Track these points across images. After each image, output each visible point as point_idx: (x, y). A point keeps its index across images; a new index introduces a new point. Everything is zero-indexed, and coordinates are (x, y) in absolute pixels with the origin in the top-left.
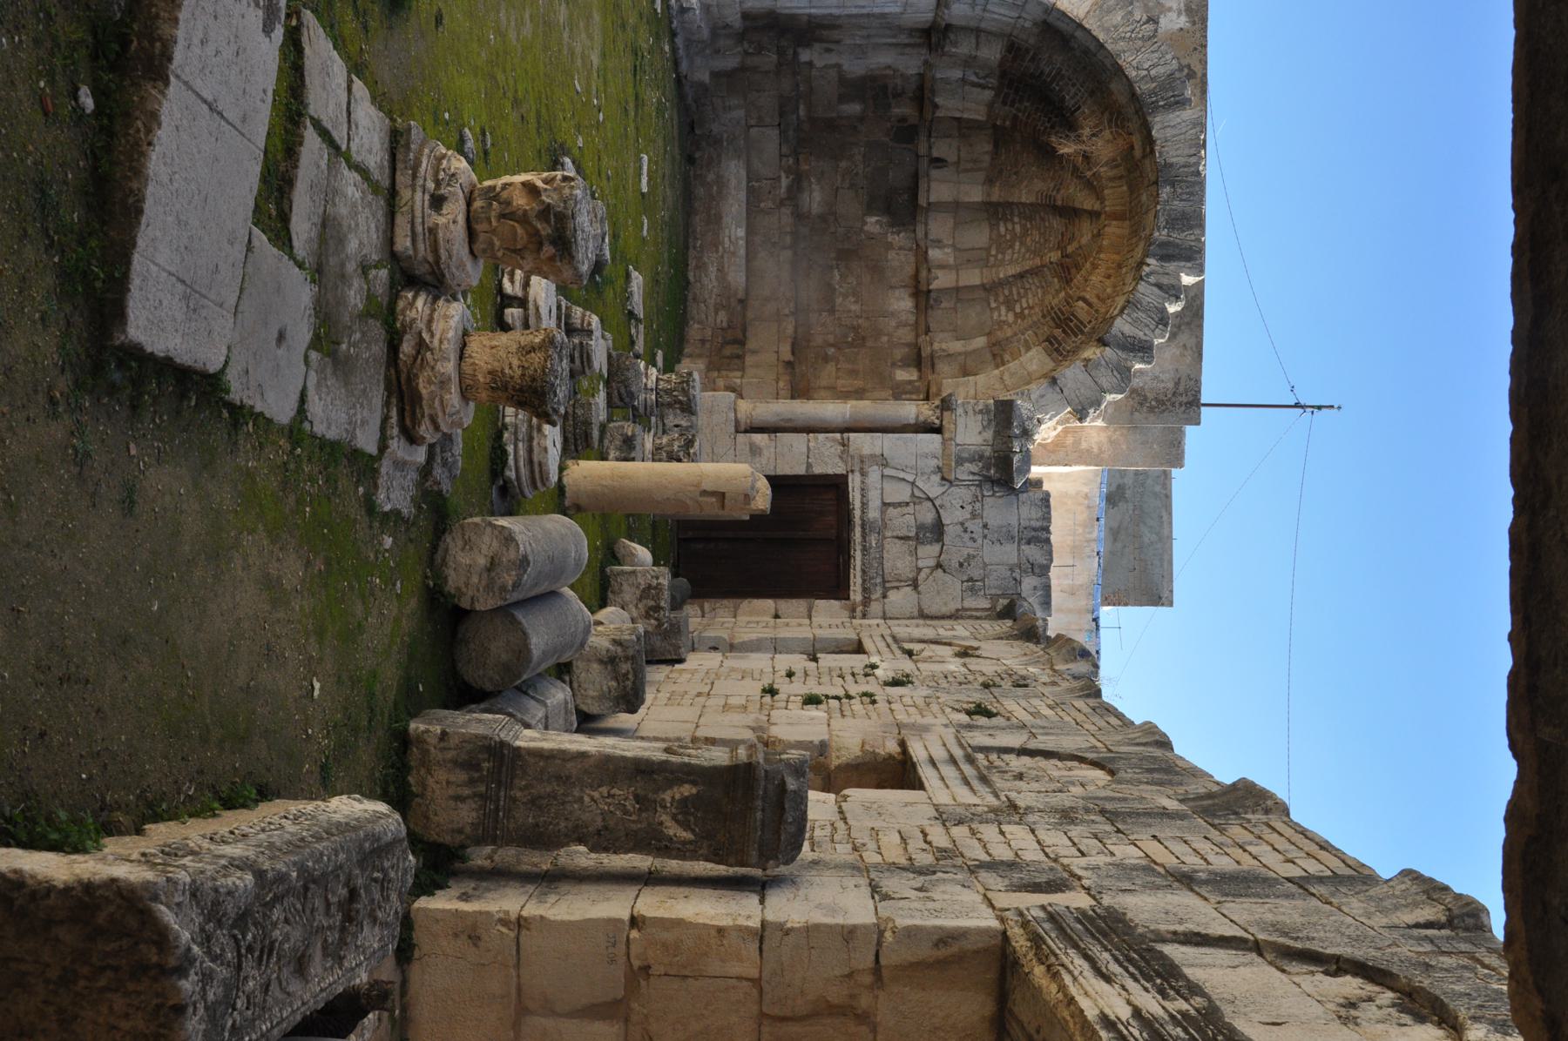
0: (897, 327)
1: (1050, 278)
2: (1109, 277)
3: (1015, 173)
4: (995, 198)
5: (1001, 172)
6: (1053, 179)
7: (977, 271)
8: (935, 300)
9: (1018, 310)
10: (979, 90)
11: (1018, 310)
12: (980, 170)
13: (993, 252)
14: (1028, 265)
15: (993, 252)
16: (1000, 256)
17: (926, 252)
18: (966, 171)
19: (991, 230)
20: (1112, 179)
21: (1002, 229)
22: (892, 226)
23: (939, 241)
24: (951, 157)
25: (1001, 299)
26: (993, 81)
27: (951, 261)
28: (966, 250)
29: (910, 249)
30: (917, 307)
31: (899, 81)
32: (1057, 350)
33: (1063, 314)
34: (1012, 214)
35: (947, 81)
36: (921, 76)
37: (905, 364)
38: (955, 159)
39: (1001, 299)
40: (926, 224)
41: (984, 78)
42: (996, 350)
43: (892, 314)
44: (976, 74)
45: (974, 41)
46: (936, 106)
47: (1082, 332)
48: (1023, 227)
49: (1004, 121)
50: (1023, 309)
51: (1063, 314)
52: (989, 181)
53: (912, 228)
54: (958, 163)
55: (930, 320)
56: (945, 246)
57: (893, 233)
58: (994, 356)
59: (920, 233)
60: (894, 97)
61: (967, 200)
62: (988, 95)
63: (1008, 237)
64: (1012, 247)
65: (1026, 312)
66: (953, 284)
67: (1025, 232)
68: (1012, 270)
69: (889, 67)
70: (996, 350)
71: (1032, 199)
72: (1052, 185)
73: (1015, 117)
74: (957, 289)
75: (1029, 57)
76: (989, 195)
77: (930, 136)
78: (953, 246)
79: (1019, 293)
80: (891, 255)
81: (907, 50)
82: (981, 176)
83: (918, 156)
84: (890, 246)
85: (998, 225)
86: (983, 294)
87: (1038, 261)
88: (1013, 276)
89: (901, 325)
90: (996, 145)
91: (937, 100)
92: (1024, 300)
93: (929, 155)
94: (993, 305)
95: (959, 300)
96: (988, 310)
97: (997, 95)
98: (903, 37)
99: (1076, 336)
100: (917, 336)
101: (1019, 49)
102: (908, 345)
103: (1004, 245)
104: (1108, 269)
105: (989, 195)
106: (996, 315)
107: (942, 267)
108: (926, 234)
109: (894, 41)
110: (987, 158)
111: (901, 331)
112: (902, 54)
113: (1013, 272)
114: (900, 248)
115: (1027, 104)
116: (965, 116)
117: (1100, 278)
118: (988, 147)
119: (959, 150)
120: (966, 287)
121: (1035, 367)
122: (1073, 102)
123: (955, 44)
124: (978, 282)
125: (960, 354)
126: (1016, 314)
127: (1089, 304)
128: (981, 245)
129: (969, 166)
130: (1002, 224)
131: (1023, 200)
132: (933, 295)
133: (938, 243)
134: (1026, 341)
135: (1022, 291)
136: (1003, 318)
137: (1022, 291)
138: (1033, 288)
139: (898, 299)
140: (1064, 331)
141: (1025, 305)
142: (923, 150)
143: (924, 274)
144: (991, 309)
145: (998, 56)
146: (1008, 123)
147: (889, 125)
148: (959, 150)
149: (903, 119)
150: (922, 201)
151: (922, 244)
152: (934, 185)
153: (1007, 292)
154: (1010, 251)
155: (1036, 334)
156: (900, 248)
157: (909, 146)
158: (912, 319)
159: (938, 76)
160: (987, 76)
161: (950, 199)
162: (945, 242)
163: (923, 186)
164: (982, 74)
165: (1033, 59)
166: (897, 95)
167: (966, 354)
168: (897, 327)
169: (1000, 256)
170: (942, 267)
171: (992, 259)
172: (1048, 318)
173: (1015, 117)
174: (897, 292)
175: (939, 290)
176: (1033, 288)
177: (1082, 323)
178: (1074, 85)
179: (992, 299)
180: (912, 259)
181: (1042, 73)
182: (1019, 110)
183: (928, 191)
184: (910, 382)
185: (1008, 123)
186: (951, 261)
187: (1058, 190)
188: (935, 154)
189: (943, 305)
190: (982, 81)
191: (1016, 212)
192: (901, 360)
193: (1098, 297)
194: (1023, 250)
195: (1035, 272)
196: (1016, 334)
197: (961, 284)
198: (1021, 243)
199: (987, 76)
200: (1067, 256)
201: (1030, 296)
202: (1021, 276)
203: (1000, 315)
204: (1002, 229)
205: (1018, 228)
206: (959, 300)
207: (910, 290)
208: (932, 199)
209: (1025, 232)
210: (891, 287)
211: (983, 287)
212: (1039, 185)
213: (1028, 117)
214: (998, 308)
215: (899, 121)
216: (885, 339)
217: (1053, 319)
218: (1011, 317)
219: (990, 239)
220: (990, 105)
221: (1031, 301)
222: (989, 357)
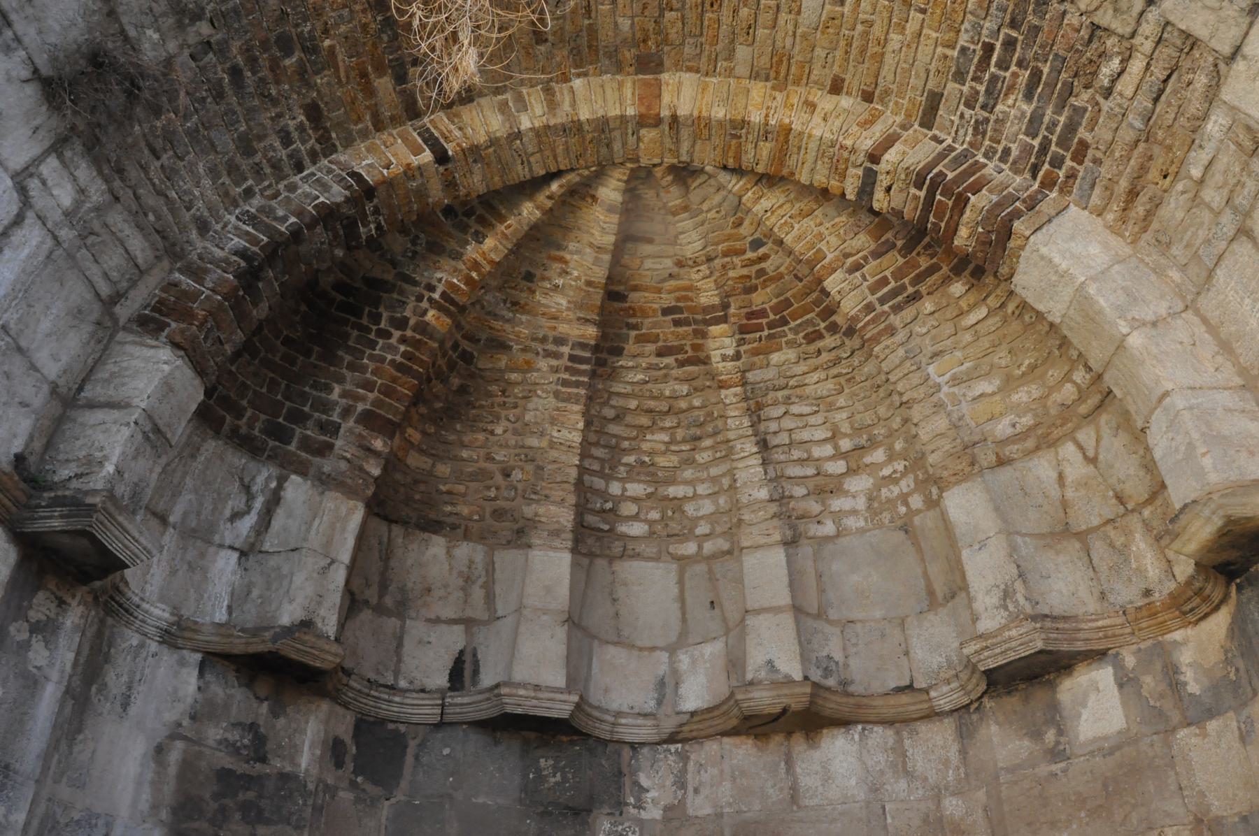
0: (909, 774)
1: (770, 374)
2: (811, 106)
3: (507, 475)
4: (566, 517)
5: (498, 514)
6: (529, 367)
7: (750, 561)
8: (827, 672)
9: (839, 467)
10: (280, 513)
11: (839, 467)
12: (490, 568)
13: (690, 548)
14: (737, 423)
15: (690, 548)
16: (702, 529)
17: (693, 714)
18: (490, 598)
19: (637, 556)
20: (552, 105)
21: (637, 529)
22: (620, 805)
23: (661, 684)
24: (452, 640)
25: (815, 508)
26: (264, 476)
27: (712, 650)
28: (684, 620)
29: (683, 757)
30: (844, 723)
31: (214, 733)
32: (1032, 203)
33: (884, 281)
34: (605, 495)
35: (239, 598)
36: (213, 660)
37: (1054, 716)
38: (459, 629)
39: (815, 508)
40: (619, 714)
41: (250, 497)
42: (986, 456)
43: (875, 789)
44: (236, 516)
45: (99, 415)
46: (306, 624)
47: (965, 155)
48: (633, 473)
49: (369, 451)
50: (839, 455)
51: (884, 281)
52: (521, 536)
53: (626, 752)
54: (468, 623)
55: (877, 687)
56: (675, 672)
57: (639, 807)
58: (1002, 462)
59: (641, 731)
60: (263, 759)
61: (564, 591)
62: (297, 490)
63: (655, 515)
64: (677, 504)
65: (846, 444)
66: (788, 619)
67: (646, 470)
68: (750, 469)
69: (160, 750)
70: (986, 456)
71: (575, 415)
72: (543, 364)
73: (368, 419)
74: (798, 610)
75: (187, 282)
76: (556, 533)
77: (392, 688)
78: (672, 650)
79: (801, 461)
80: (699, 806)
81: (115, 679)
82: (505, 558)
83: (440, 725)
84: (674, 813)
85: (624, 536)
86: (806, 550)
87: (730, 395)
88: (765, 463)
89: (901, 765)
90: (433, 526)
91: (285, 620)
92: (817, 452)
93: (442, 693)
94: (829, 528)
95: (820, 615)
96: (844, 541)
97: (302, 470)
98: (38, 655)
99: (977, 167)
100: (932, 715)
101: (160, 307)
102: (964, 734)
103: (675, 527)
104: (788, 105)
105: (556, 533)
106: (852, 523)
107: (735, 663)
108: (645, 715)
109: (50, 695)
110: (465, 550)
111: (919, 758)
112: (125, 706)
113: (756, 460)
114: (681, 784)
115: (337, 389)
116: (345, 557)
117: (817, 119)
118: (437, 546)
119: (437, 621)
120: (792, 584)
121: (1094, 249)
122: (336, 188)
123: (92, 463)
124: (778, 556)
125: (1013, 549)
126: (851, 472)
127: (889, 141)
128: (673, 577)
129: (478, 594)
130: (623, 528)
131: (576, 438)
132: (816, 675)
133: (666, 687)
134: (956, 381)
135: (796, 454)
136: (861, 503)
137: (796, 454)
138: (788, 423)
139: (827, 778)
140: (976, 189)
141: (828, 450)
142: (427, 711)
143: (764, 700)
144: (838, 536)
145: (165, 353)
146: (378, 444)
147: (345, 796)
148: (437, 621)
149: (336, 750)
150: (561, 708)
151: (669, 725)
152: (519, 675)
153: (799, 491)
154: (690, 508)
155: (935, 355)
156: (681, 784)
157: (412, 745)
158: (879, 734)
159: (221, 616)
160: (247, 488)
161: (561, 633)
162: (663, 669)
163: (520, 703)
164: (236, 502)
165: (197, 274)
166: (259, 748)
167: (1009, 531)
168: (909, 774)
169: (702, 529)
170: (735, 663)
171: (708, 547)
172: (896, 320)
173: (368, 419)
174: (808, 779)
175: (804, 659)
176: (788, 423)
177: (941, 156)
178: (292, 188)
179: (815, 530)
180: (712, 747)
181: (242, 253)
182: (346, 412)
183: (537, 687)
184: (1125, 682)
185: (378, 444)
186: (712, 650)
187: (560, 341)
188: (442, 680)
189: (838, 656)
190: (258, 504)
191: (599, 483)
192: (1037, 735)
193: (867, 123)
194: (688, 474)
195: (755, 412)
196: (939, 406)
197: (784, 599)
198: (672, 481)
199: (247, 488)
200: (725, 306)
201: (805, 435)
202: (764, 445)
203: (854, 512)
204: (637, 529)
205: (635, 489)
206: (820, 615)
207: (799, 744)
208: (561, 682)
209: (646, 470)
210: (794, 795)
211: (790, 543)
212: (543, 404)
213: (369, 386)
214: (838, 516)
215: (339, 764)
216: (953, 806)
217: (897, 309)
218: (860, 484)
219: (657, 559)
220: (325, 482)
221: (820, 434)
222: (1005, 474)
